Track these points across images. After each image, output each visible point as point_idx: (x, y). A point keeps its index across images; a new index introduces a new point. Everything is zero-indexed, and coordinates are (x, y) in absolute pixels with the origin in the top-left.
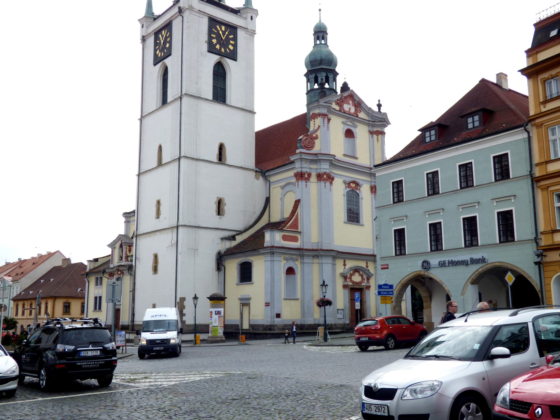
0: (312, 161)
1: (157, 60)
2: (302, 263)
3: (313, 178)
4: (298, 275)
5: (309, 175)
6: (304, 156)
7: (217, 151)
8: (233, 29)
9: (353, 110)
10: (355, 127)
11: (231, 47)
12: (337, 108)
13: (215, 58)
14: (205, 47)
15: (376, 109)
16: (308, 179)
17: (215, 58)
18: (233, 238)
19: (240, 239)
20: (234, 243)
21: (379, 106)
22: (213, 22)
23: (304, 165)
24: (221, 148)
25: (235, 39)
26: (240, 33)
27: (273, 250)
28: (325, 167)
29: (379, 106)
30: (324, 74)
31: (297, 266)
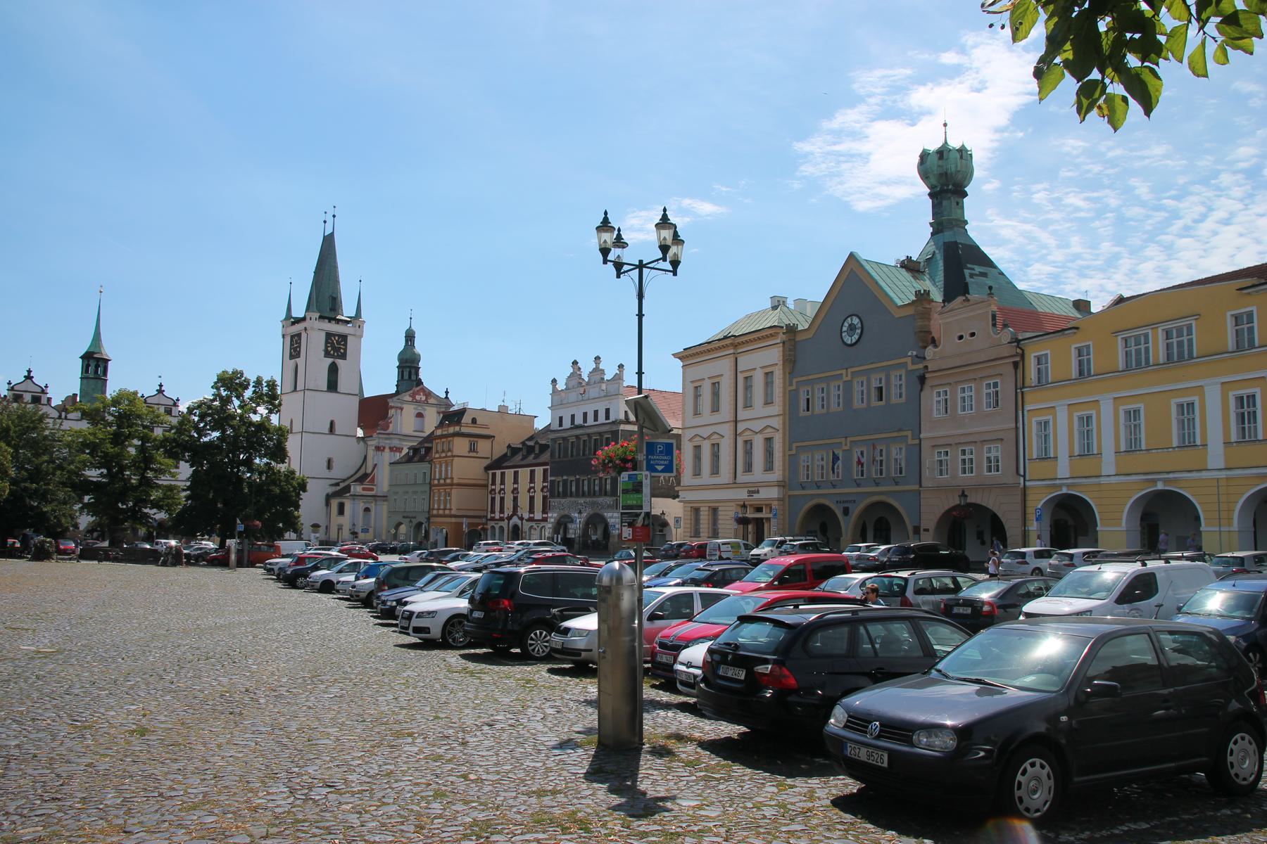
0: (386, 439)
1: (292, 357)
2: (376, 505)
3: (387, 450)
4: (373, 513)
5: (384, 448)
6: (380, 436)
7: (328, 426)
8: (344, 338)
9: (424, 398)
10: (425, 410)
11: (342, 351)
12: (410, 399)
13: (330, 360)
14: (323, 353)
15: (443, 396)
16: (383, 450)
17: (330, 360)
18: (337, 484)
19: (342, 485)
20: (338, 488)
21: (447, 392)
22: (329, 335)
23: (381, 441)
24: (332, 423)
25: (345, 345)
26: (350, 339)
27: (354, 496)
28: (396, 443)
29: (447, 392)
30: (408, 370)
31: (372, 506)
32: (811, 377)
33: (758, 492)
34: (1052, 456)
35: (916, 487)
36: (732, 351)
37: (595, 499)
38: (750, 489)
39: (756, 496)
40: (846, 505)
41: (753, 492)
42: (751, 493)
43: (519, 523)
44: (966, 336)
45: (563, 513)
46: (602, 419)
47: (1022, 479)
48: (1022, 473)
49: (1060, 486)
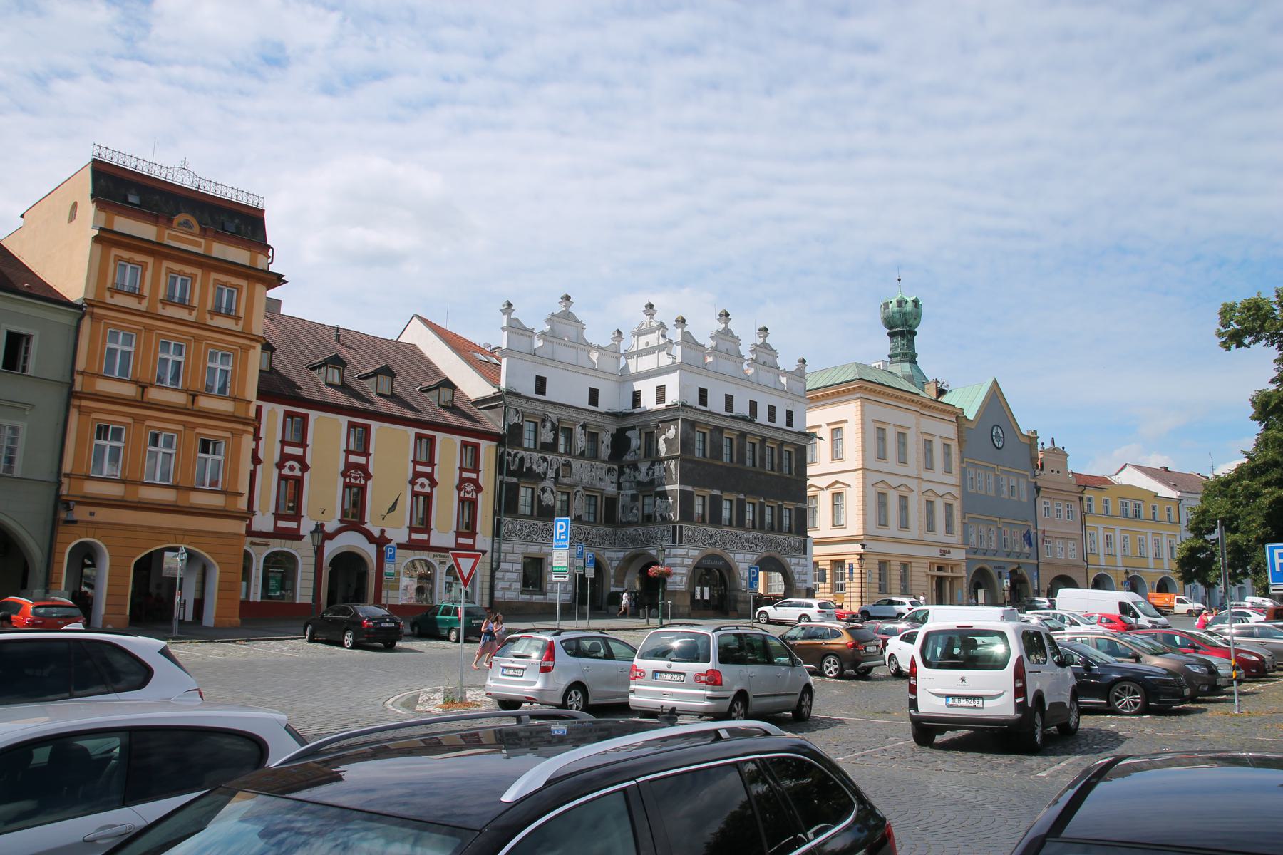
32: (976, 462)
33: (949, 552)
34: (1096, 552)
35: (1036, 562)
36: (918, 409)
37: (771, 536)
38: (943, 549)
39: (947, 556)
40: (1000, 570)
41: (945, 552)
42: (943, 552)
43: (370, 551)
44: (1055, 472)
45: (710, 550)
46: (781, 421)
47: (1086, 564)
48: (1085, 559)
49: (1101, 569)
